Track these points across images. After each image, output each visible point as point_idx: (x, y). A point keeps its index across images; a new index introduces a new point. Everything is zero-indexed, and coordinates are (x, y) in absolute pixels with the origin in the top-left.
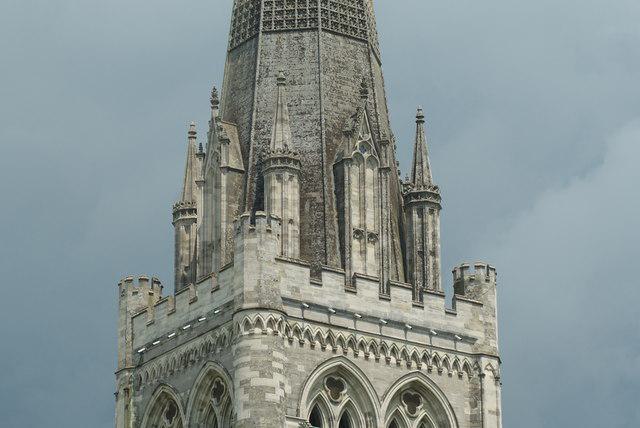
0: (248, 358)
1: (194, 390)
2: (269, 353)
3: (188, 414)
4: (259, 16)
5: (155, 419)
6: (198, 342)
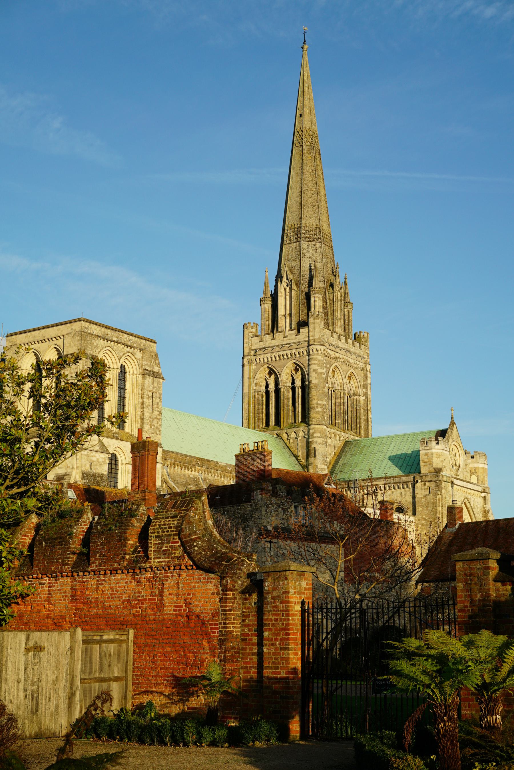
6: (289, 352)
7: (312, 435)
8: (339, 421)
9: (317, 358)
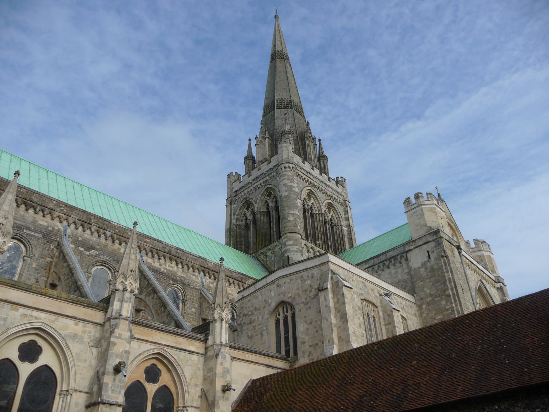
0: (286, 177)
1: (260, 196)
2: (293, 176)
3: (257, 204)
4: (274, 105)
5: (241, 211)
7: (285, 244)
8: (320, 242)
9: (286, 174)
